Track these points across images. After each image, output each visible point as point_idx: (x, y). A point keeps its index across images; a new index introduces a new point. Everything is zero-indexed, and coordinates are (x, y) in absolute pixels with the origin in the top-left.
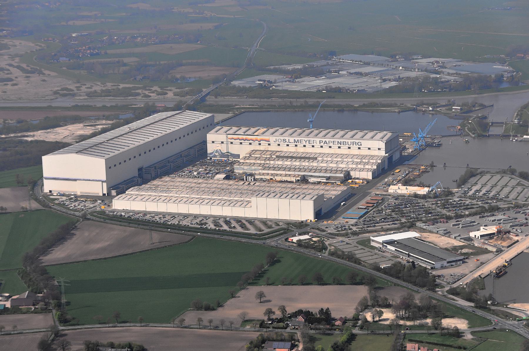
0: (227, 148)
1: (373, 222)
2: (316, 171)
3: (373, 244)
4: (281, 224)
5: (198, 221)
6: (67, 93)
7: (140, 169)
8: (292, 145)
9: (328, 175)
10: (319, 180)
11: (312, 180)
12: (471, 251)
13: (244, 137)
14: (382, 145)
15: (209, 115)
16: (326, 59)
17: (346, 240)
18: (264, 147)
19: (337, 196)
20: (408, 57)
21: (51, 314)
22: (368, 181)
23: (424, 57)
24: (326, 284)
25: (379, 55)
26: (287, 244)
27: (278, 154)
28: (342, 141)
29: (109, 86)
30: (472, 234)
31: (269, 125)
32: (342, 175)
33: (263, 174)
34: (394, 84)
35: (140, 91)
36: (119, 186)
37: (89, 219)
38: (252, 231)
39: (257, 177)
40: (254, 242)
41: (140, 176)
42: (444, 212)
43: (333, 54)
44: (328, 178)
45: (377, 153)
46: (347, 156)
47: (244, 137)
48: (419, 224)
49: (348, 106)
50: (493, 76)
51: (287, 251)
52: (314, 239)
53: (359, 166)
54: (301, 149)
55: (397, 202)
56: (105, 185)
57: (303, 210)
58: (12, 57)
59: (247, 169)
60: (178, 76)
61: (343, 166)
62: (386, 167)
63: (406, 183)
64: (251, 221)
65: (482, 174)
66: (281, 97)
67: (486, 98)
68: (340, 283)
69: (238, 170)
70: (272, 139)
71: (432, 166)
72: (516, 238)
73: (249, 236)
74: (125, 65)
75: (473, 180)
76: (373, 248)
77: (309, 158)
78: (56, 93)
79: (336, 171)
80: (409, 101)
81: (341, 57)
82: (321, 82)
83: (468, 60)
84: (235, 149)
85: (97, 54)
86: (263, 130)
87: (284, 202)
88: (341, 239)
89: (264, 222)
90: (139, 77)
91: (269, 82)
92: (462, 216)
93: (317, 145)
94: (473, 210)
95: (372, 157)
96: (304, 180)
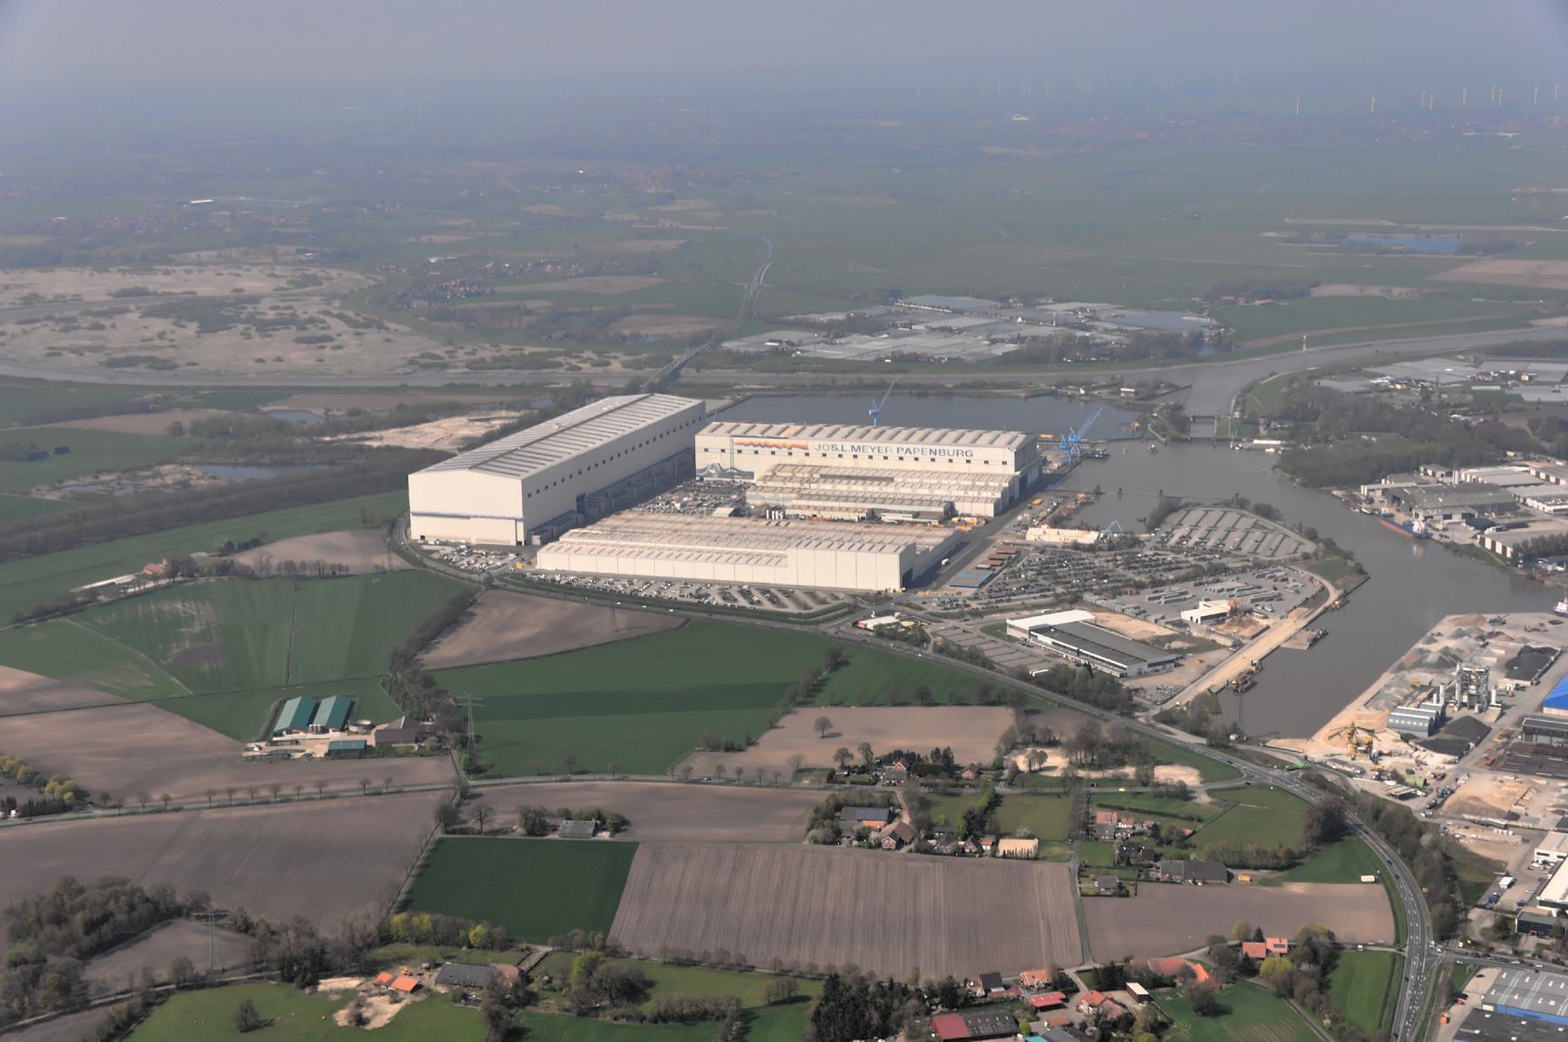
0: (732, 461)
1: (1004, 593)
2: (893, 501)
3: (1010, 632)
4: (841, 596)
5: (693, 590)
6: (432, 363)
7: (580, 499)
8: (848, 455)
9: (916, 509)
10: (900, 517)
11: (886, 518)
12: (1187, 645)
13: (763, 441)
14: (1010, 457)
15: (695, 402)
16: (885, 303)
17: (963, 625)
18: (798, 457)
19: (937, 547)
20: (1029, 301)
21: (449, 758)
22: (987, 521)
23: (1058, 300)
24: (936, 705)
25: (978, 297)
26: (858, 632)
27: (823, 471)
28: (938, 447)
29: (506, 349)
30: (1186, 615)
31: (805, 419)
32: (941, 510)
33: (800, 507)
34: (1011, 347)
35: (560, 359)
36: (546, 529)
37: (497, 587)
38: (792, 608)
39: (788, 512)
40: (797, 628)
41: (580, 509)
42: (1130, 574)
43: (896, 294)
44: (916, 515)
45: (1000, 469)
46: (949, 475)
47: (763, 441)
48: (1088, 597)
49: (933, 386)
50: (1185, 334)
51: (862, 644)
52: (905, 624)
53: (970, 493)
54: (864, 463)
55: (1044, 558)
56: (521, 525)
57: (878, 571)
58: (329, 299)
59: (770, 498)
60: (626, 332)
61: (940, 493)
62: (1017, 496)
63: (1057, 523)
64: (787, 592)
65: (1189, 507)
66: (814, 371)
67: (1176, 373)
68: (961, 703)
69: (754, 500)
70: (813, 444)
71: (1098, 493)
72: (1264, 623)
73: (784, 617)
74: (529, 312)
75: (1173, 518)
76: (1012, 639)
77: (880, 479)
78: (412, 362)
79: (931, 503)
80: (1043, 379)
81: (912, 299)
82: (881, 345)
83: (1136, 307)
84: (744, 462)
85: (478, 294)
86: (794, 428)
87: (846, 557)
88: (952, 623)
89: (811, 593)
90: (558, 334)
91: (789, 343)
92: (1163, 583)
93: (893, 456)
94: (1182, 572)
95: (993, 476)
96: (873, 518)
